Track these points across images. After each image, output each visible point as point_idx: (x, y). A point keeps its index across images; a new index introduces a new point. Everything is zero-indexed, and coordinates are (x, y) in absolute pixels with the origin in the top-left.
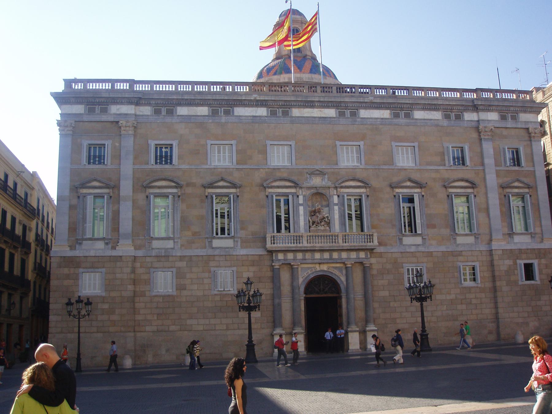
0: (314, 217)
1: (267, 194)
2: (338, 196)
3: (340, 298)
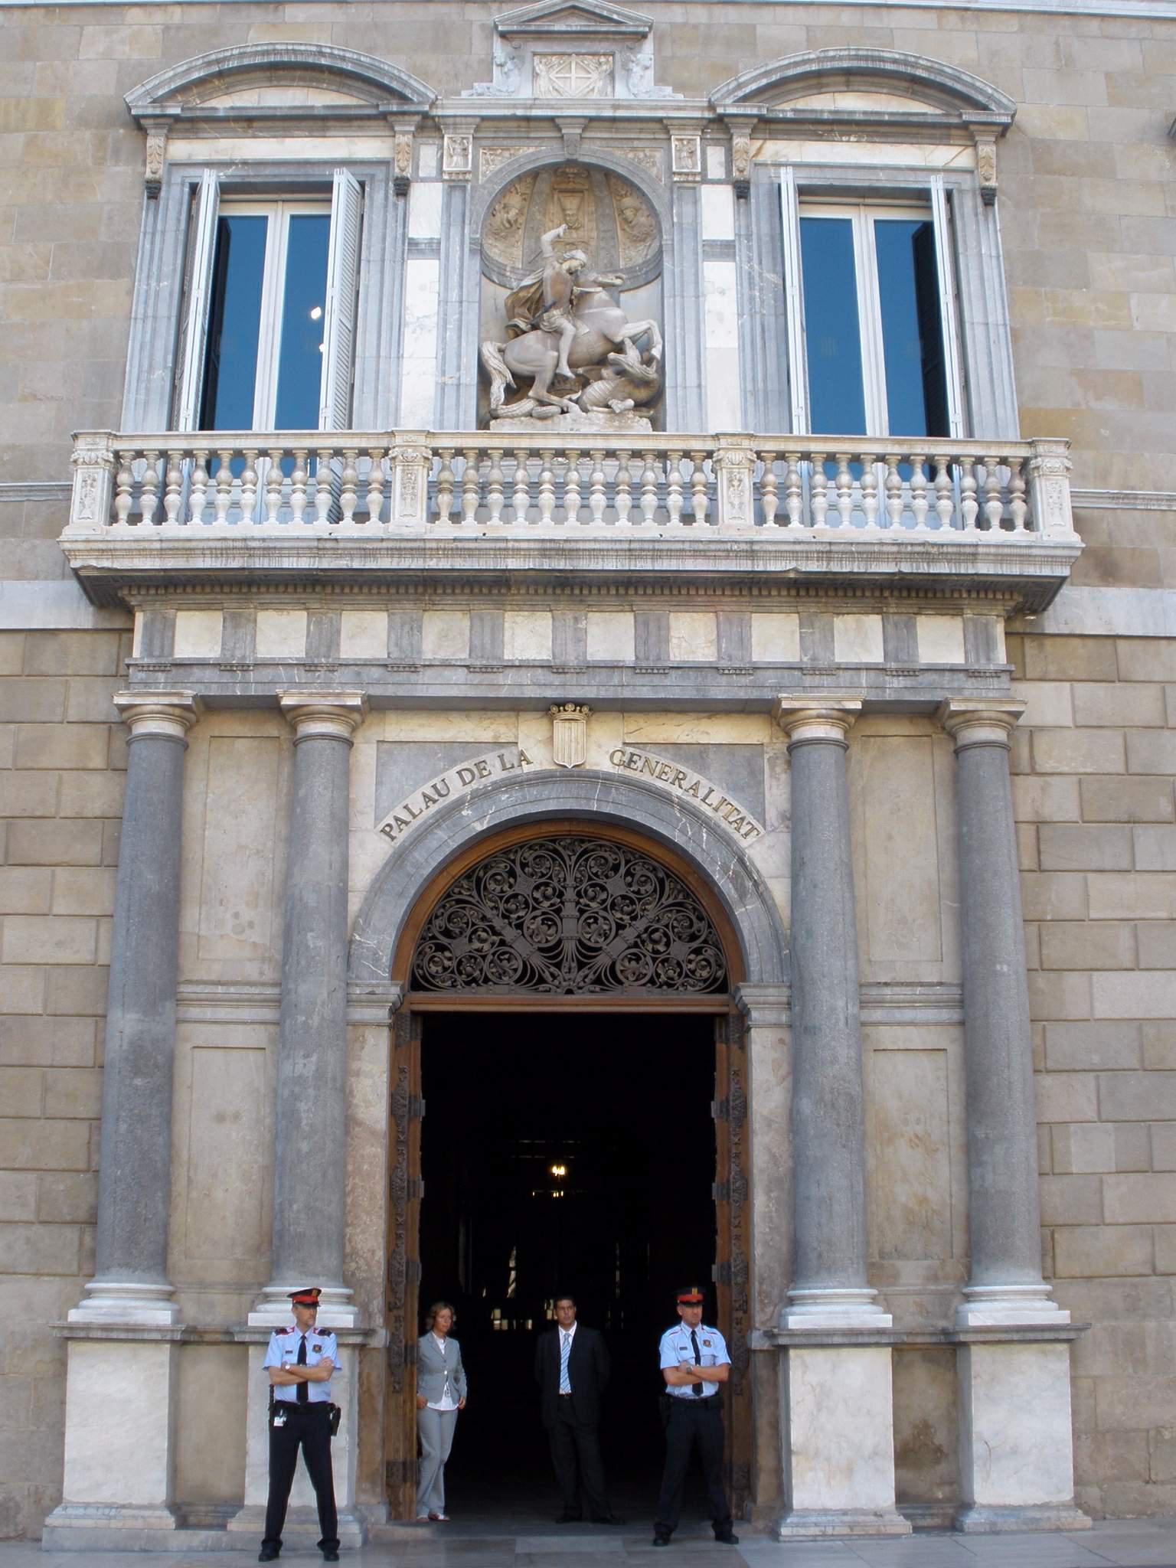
0: (532, 339)
1: (153, 168)
2: (742, 191)
3: (735, 1023)
